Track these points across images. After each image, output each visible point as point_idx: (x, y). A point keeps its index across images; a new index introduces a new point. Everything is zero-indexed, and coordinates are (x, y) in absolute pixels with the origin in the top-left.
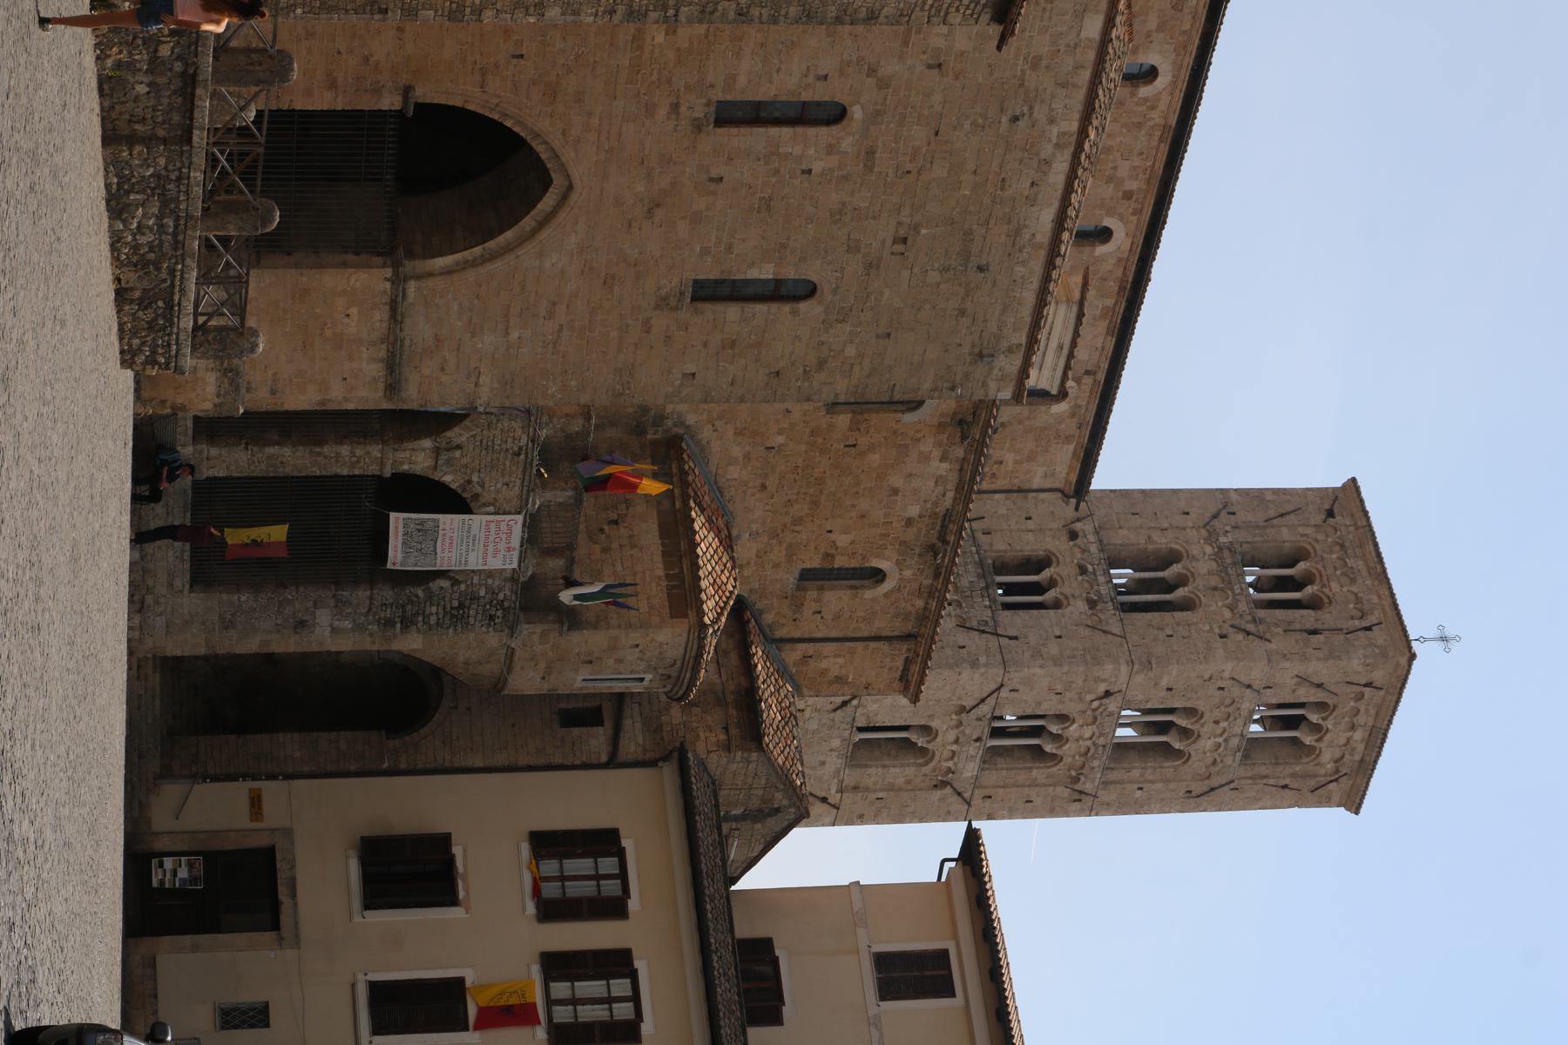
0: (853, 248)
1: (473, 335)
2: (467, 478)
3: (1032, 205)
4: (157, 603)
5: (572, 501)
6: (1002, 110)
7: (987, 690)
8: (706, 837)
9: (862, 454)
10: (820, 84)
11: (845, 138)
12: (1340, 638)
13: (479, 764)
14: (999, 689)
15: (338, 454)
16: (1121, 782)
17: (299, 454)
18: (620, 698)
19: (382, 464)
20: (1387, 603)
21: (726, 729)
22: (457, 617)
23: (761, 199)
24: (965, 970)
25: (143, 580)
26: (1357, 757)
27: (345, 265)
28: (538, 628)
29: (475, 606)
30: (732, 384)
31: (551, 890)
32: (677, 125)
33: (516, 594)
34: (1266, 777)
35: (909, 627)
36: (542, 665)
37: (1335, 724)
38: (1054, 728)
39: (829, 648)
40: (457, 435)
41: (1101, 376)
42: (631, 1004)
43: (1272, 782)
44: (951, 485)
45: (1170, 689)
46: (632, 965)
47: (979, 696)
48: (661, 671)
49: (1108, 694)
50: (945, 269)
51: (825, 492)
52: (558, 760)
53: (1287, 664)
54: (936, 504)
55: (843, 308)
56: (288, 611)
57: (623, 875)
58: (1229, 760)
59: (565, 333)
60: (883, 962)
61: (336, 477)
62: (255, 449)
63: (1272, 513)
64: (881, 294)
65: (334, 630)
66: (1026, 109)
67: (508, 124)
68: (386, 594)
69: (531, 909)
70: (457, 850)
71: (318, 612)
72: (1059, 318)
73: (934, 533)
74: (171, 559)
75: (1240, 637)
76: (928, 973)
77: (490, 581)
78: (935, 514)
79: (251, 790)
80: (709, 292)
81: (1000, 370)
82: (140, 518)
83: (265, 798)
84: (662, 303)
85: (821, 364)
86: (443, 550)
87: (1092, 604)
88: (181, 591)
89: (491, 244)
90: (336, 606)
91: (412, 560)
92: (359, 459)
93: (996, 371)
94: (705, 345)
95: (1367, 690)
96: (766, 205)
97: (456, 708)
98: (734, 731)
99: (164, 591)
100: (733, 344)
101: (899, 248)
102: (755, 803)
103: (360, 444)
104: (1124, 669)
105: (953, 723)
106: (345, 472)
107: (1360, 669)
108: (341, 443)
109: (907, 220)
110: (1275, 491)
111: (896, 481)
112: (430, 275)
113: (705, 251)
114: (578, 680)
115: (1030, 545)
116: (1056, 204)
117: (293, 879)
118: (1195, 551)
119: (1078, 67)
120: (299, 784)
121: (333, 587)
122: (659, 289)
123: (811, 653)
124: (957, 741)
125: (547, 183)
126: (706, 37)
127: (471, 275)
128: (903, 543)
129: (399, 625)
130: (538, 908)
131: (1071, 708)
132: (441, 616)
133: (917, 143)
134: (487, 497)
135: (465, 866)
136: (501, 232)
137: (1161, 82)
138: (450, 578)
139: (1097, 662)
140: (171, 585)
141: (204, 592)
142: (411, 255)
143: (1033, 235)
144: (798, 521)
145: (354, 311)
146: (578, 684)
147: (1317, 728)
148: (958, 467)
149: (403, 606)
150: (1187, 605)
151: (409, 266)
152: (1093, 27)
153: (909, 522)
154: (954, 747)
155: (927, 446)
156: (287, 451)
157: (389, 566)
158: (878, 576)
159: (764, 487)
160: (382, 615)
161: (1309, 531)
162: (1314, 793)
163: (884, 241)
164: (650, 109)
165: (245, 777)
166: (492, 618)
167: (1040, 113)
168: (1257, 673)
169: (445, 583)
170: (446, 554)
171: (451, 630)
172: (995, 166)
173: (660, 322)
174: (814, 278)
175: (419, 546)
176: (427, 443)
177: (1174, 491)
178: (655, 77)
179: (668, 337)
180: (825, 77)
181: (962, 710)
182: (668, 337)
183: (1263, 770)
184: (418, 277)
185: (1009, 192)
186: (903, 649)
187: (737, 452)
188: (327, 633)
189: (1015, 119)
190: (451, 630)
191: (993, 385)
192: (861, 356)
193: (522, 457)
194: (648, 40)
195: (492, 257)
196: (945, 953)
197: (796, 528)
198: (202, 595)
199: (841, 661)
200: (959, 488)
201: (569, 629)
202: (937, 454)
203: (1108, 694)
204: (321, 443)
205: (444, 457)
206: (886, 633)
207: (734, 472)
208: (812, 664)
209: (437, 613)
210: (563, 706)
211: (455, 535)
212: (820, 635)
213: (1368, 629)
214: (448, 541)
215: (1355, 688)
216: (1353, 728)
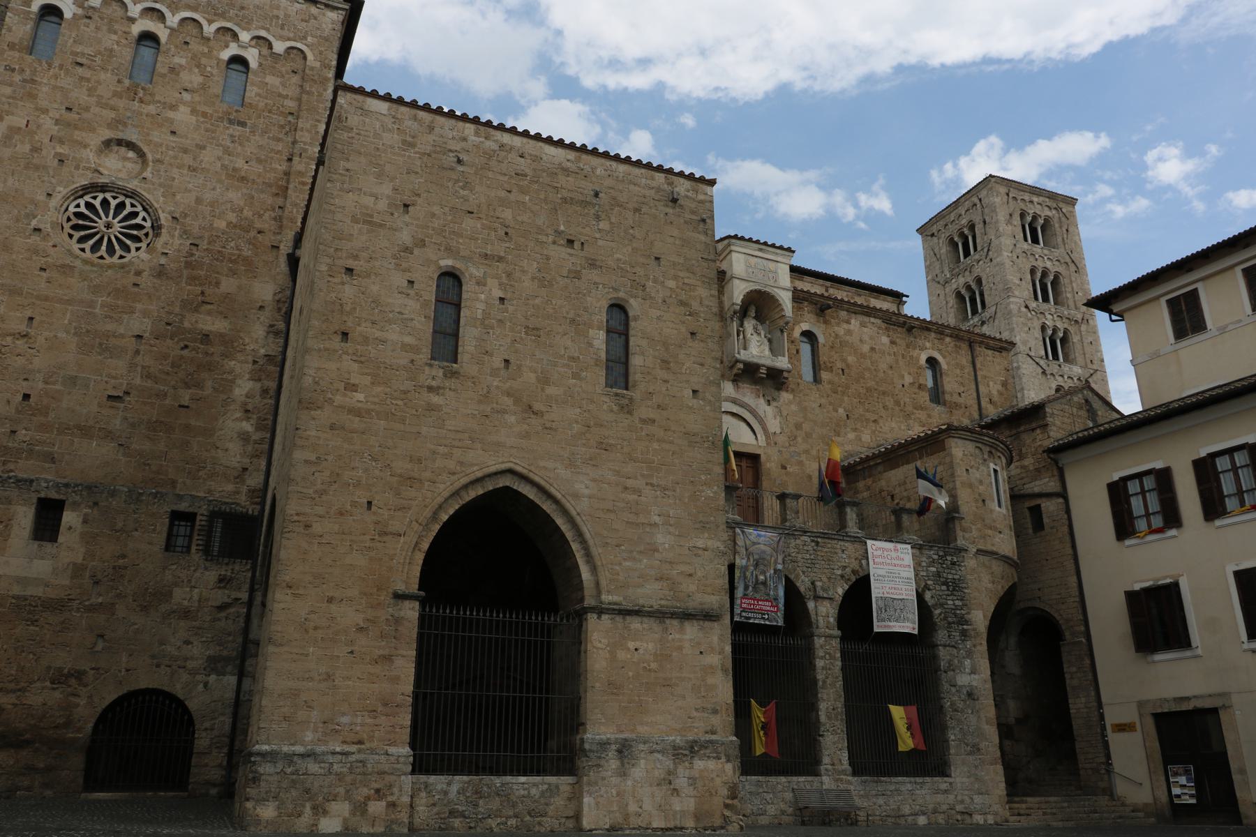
0: (576, 275)
1: (656, 550)
2: (839, 577)
3: (541, 159)
4: (962, 802)
5: (855, 509)
6: (452, 169)
7: (1031, 361)
9: (848, 366)
10: (416, 286)
11: (472, 272)
12: (986, 210)
13: (1074, 579)
14: (1030, 356)
15: (823, 668)
16: (1075, 301)
17: (825, 697)
19: (831, 637)
20: (967, 196)
21: (1033, 430)
22: (955, 587)
23: (526, 333)
25: (944, 813)
26: (1047, 200)
27: (585, 652)
28: (959, 533)
29: (945, 575)
30: (702, 365)
31: (1157, 522)
32: (450, 389)
33: (932, 546)
34: (1063, 239)
35: (965, 346)
36: (990, 532)
37: (1031, 209)
38: (1050, 332)
39: (982, 389)
40: (803, 584)
41: (828, 284)
42: (1236, 455)
43: (1065, 236)
44: (866, 319)
45: (1021, 280)
46: (1204, 458)
47: (1035, 365)
48: (986, 456)
49: (1027, 307)
50: (598, 218)
51: (876, 387)
52: (1066, 529)
53: (1001, 229)
54: (879, 328)
55: (632, 286)
56: (960, 705)
57: (1139, 476)
58: (1056, 254)
59: (655, 481)
61: (843, 669)
62: (822, 729)
63: (935, 259)
64: (618, 260)
65: (973, 672)
66: (451, 154)
67: (445, 517)
68: (941, 636)
69: (1173, 532)
70: (1137, 587)
71: (959, 683)
73: (899, 329)
74: (923, 792)
75: (990, 253)
76: (1184, 308)
77: (924, 564)
78: (886, 328)
79: (1113, 732)
81: (688, 191)
82: (889, 816)
83: (1117, 721)
84: (627, 408)
85: (682, 303)
86: (900, 594)
87: (983, 323)
88: (951, 784)
89: (569, 535)
90: (953, 670)
91: (910, 616)
92: (826, 653)
93: (689, 194)
94: (666, 381)
95: (1011, 195)
96: (533, 331)
97: (1039, 597)
98: (1034, 425)
99: (951, 797)
100: (663, 361)
101: (577, 245)
102: (1083, 413)
103: (814, 652)
104: (1012, 299)
105: (1052, 377)
106: (839, 663)
107: (1000, 198)
108: (815, 666)
109: (551, 239)
110: (926, 261)
111: (866, 348)
112: (597, 584)
113: (576, 376)
114: (1001, 512)
116: (541, 144)
117: (1175, 699)
118: (954, 286)
119: (415, 118)
120: (1104, 700)
121: (939, 673)
122: (612, 411)
123: (987, 399)
124: (1062, 376)
126: (362, 362)
127: (595, 551)
128: (908, 346)
129: (965, 627)
130: (1171, 528)
131: (1037, 325)
132: (955, 598)
133: (479, 226)
134: (855, 565)
135: (1148, 581)
136: (558, 528)
138: (923, 591)
139: (1010, 312)
140: (946, 791)
141: (950, 766)
142: (582, 599)
143: (568, 160)
144: (897, 403)
145: (631, 645)
146: (1004, 511)
147: (1035, 218)
148: (853, 315)
149: (949, 623)
151: (589, 601)
153: (892, 342)
154: (1066, 377)
155: (840, 330)
156: (823, 706)
157: (916, 632)
158: (932, 362)
159: (875, 421)
160: (958, 638)
161: (941, 241)
162: (1069, 219)
163: (571, 255)
164: (431, 408)
165: (1104, 736)
166: (953, 563)
168: (1007, 242)
169: (928, 596)
170: (904, 592)
171: (966, 591)
172: (506, 178)
173: (644, 411)
174: (605, 304)
175: (898, 611)
176: (811, 605)
177: (930, 303)
178: (400, 403)
179: (659, 406)
180: (411, 282)
181: (1044, 373)
182: (659, 406)
183: (1060, 240)
184: (599, 593)
185: (528, 171)
186: (978, 349)
187: (851, 436)
188: (976, 677)
189: (459, 161)
190: (966, 591)
191: (701, 197)
192: (675, 278)
193: (819, 540)
194: (360, 405)
195: (580, 534)
196: (1168, 301)
197: (902, 403)
198: (952, 768)
199: (991, 383)
200: (868, 315)
201: (958, 513)
202: (845, 326)
203: (1027, 307)
204: (815, 681)
205: (821, 593)
206: (970, 358)
207: (866, 438)
208: (996, 399)
209: (953, 600)
210: (1030, 531)
211: (888, 586)
212: (975, 394)
213: (980, 200)
214: (893, 591)
215: (1010, 200)
216: (1031, 202)
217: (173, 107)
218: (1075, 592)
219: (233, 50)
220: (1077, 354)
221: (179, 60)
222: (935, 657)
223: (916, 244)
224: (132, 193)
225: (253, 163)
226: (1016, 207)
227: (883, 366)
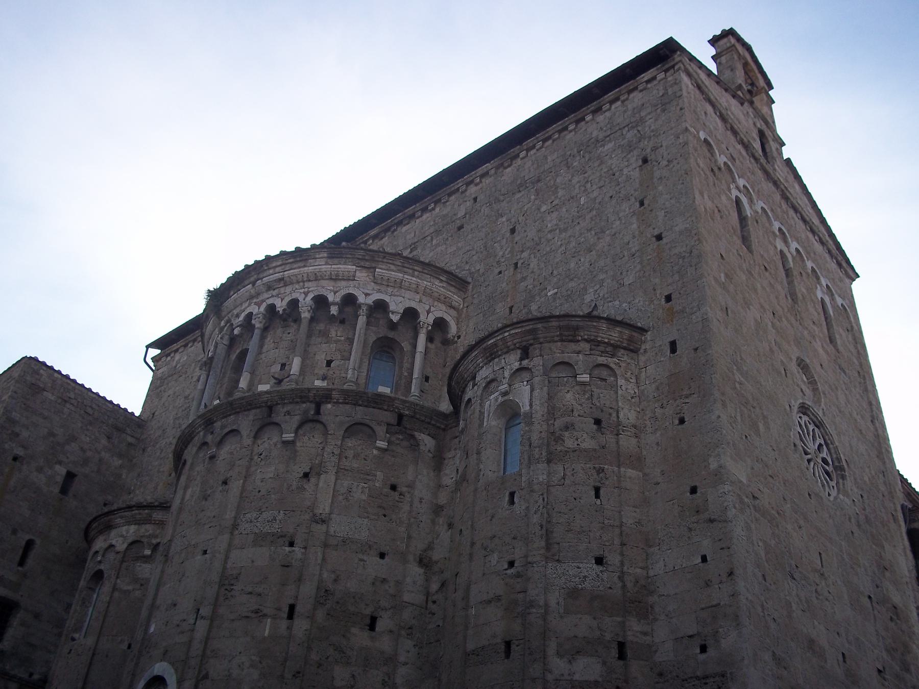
224: (820, 422)
225: (859, 417)
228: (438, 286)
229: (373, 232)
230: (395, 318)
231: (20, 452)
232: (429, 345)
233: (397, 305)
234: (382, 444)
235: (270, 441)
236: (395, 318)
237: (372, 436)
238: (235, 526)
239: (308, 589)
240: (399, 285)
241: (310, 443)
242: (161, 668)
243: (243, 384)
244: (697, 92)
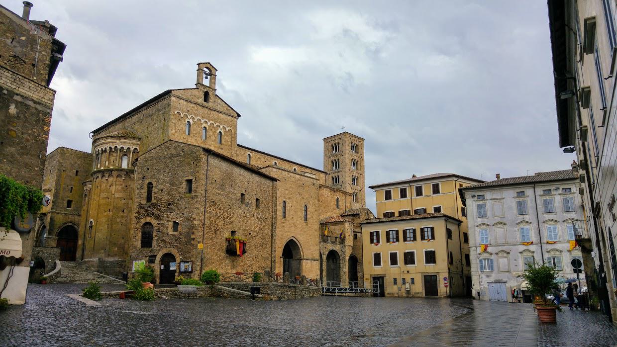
0: (301, 201)
8: (371, 221)
11: (287, 201)
18: (354, 232)
22: (344, 252)
24: (387, 188)
35: (344, 196)
60: (387, 199)
72: (307, 175)
80: (306, 219)
84: (307, 225)
114: (352, 237)
115: (331, 179)
125: (292, 240)
137: (276, 162)
150: (339, 160)
151: (302, 258)
152: (274, 170)
158: (338, 198)
162: (362, 144)
164: (283, 226)
167: (284, 176)
168: (347, 152)
217: (211, 146)
218: (361, 253)
219: (219, 130)
220: (359, 184)
221: (211, 134)
222: (340, 265)
223: (322, 143)
226: (350, 141)
227: (329, 200)
228: (134, 141)
229: (128, 116)
230: (125, 151)
231: (64, 169)
232: (134, 154)
233: (125, 148)
234: (123, 178)
235: (104, 179)
236: (125, 151)
237: (122, 177)
238: (100, 196)
239: (111, 207)
240: (125, 143)
241: (111, 179)
242: (92, 220)
243: (99, 167)
244: (178, 99)
